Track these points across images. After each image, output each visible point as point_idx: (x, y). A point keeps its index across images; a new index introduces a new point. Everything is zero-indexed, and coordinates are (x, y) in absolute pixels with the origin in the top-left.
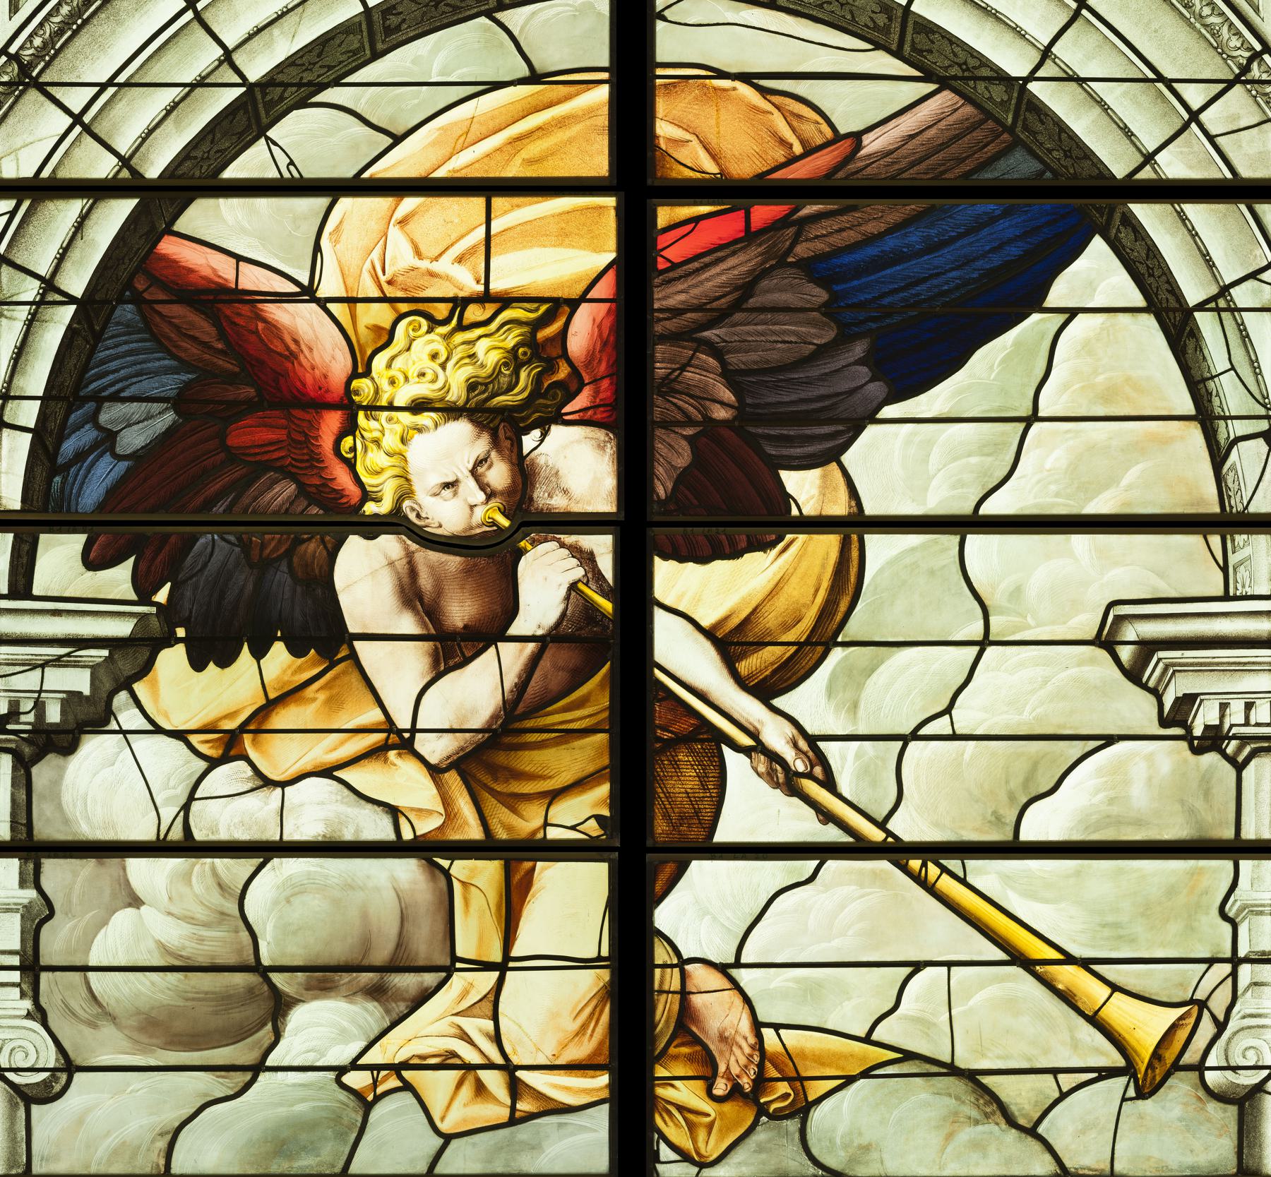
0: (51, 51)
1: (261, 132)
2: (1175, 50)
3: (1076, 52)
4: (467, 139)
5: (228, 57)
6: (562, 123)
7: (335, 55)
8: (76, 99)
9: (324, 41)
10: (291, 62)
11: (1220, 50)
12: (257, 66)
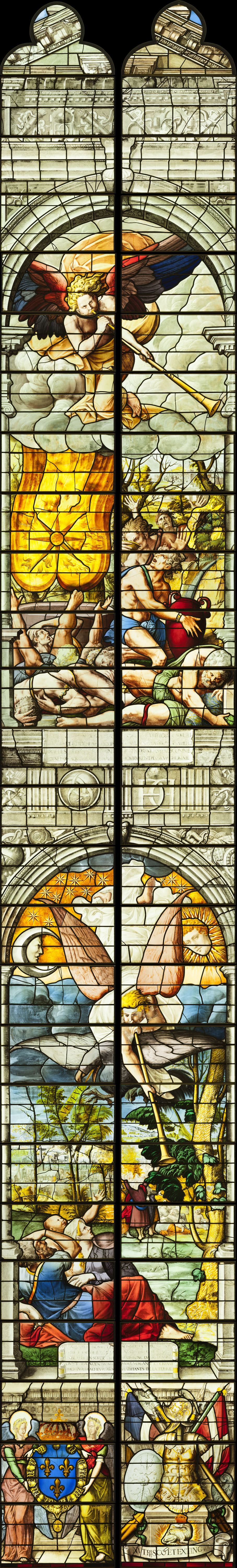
0: (13, 228)
1: (51, 242)
2: (216, 227)
3: (198, 228)
4: (88, 243)
5: (45, 229)
6: (105, 241)
7: (64, 228)
8: (17, 236)
9: (62, 226)
10: (56, 230)
11: (224, 228)
12: (50, 230)
